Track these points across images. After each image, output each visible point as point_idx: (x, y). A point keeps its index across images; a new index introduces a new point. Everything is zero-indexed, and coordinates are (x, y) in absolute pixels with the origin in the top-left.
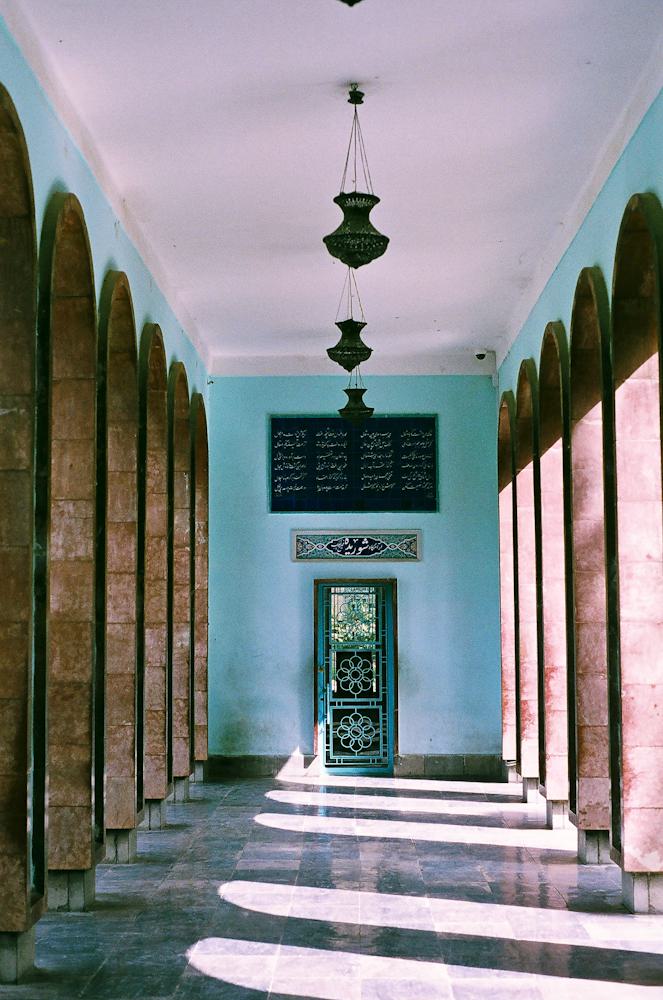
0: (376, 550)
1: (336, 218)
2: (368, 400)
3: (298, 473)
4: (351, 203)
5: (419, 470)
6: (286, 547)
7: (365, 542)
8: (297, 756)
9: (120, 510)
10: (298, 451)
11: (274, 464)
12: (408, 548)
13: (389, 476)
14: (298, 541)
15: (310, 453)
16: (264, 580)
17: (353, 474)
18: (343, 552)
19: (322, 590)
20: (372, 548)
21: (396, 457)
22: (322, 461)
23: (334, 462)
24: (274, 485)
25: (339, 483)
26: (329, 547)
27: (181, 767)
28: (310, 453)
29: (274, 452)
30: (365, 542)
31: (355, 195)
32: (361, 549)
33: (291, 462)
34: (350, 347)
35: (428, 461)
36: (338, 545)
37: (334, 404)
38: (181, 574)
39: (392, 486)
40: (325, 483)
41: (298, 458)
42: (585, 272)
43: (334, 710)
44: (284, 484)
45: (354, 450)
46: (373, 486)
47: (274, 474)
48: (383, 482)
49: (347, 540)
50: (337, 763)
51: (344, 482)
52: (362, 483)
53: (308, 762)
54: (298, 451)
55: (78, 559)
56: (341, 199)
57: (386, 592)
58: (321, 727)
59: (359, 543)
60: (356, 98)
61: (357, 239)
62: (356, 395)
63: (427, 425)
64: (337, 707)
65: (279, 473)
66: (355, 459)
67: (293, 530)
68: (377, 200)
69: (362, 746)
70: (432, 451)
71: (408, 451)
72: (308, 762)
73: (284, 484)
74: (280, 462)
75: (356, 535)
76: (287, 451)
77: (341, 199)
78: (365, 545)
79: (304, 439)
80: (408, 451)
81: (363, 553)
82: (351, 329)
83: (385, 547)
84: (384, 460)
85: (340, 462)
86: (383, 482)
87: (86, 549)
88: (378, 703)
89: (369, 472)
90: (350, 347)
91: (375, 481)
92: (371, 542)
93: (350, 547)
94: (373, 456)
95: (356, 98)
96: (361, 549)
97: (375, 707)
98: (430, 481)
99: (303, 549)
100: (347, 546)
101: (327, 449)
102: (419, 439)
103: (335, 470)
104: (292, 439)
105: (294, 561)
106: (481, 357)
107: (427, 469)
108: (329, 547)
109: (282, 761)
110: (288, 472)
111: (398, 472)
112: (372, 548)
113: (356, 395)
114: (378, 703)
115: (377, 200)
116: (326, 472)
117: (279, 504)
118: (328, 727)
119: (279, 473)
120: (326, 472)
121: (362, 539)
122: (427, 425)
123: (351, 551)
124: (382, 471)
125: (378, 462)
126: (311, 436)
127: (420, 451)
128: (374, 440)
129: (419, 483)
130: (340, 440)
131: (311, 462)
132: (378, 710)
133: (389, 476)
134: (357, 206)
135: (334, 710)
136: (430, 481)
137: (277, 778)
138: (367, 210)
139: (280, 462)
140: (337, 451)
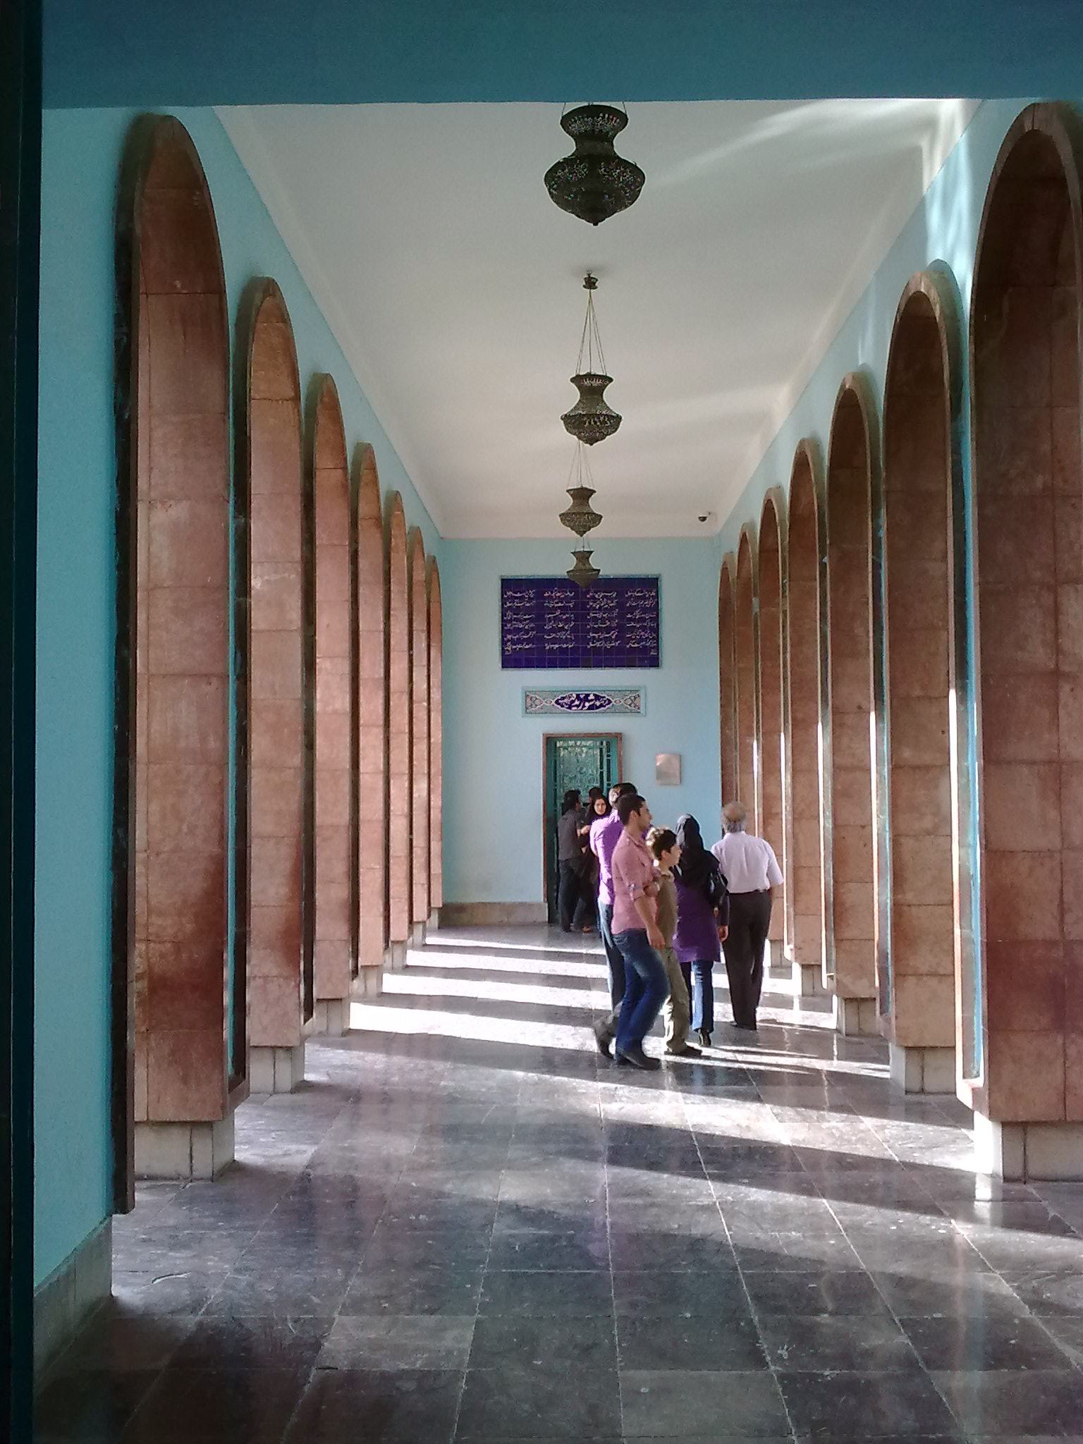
0: (601, 706)
1: (572, 397)
2: (594, 562)
4: (587, 383)
5: (644, 628)
7: (591, 697)
9: (371, 668)
10: (528, 611)
11: (504, 622)
12: (632, 702)
13: (614, 634)
15: (539, 614)
17: (580, 632)
18: (570, 708)
19: (551, 742)
21: (621, 616)
24: (504, 643)
25: (567, 641)
26: (557, 702)
27: (420, 912)
28: (539, 614)
30: (591, 697)
31: (590, 376)
32: (587, 704)
34: (581, 510)
37: (561, 566)
38: (420, 728)
40: (554, 641)
42: (802, 443)
45: (581, 611)
46: (598, 644)
47: (504, 632)
54: (528, 611)
55: (335, 712)
56: (577, 380)
59: (586, 698)
60: (590, 283)
61: (592, 419)
62: (583, 557)
63: (651, 584)
68: (611, 380)
70: (656, 609)
71: (632, 610)
76: (517, 611)
77: (577, 380)
80: (632, 610)
81: (590, 708)
82: (583, 495)
83: (610, 702)
85: (567, 621)
87: (344, 703)
89: (596, 631)
90: (581, 510)
93: (577, 703)
95: (590, 283)
96: (587, 704)
99: (531, 703)
101: (556, 609)
102: (643, 598)
104: (522, 598)
106: (703, 519)
108: (557, 702)
110: (518, 630)
111: (621, 629)
112: (598, 703)
113: (583, 557)
115: (611, 380)
116: (553, 630)
117: (511, 661)
119: (509, 632)
120: (553, 630)
122: (651, 584)
124: (608, 629)
125: (603, 620)
126: (540, 596)
127: (644, 610)
128: (601, 601)
130: (568, 599)
131: (540, 618)
133: (614, 634)
134: (591, 387)
138: (602, 388)
139: (511, 621)
140: (564, 609)
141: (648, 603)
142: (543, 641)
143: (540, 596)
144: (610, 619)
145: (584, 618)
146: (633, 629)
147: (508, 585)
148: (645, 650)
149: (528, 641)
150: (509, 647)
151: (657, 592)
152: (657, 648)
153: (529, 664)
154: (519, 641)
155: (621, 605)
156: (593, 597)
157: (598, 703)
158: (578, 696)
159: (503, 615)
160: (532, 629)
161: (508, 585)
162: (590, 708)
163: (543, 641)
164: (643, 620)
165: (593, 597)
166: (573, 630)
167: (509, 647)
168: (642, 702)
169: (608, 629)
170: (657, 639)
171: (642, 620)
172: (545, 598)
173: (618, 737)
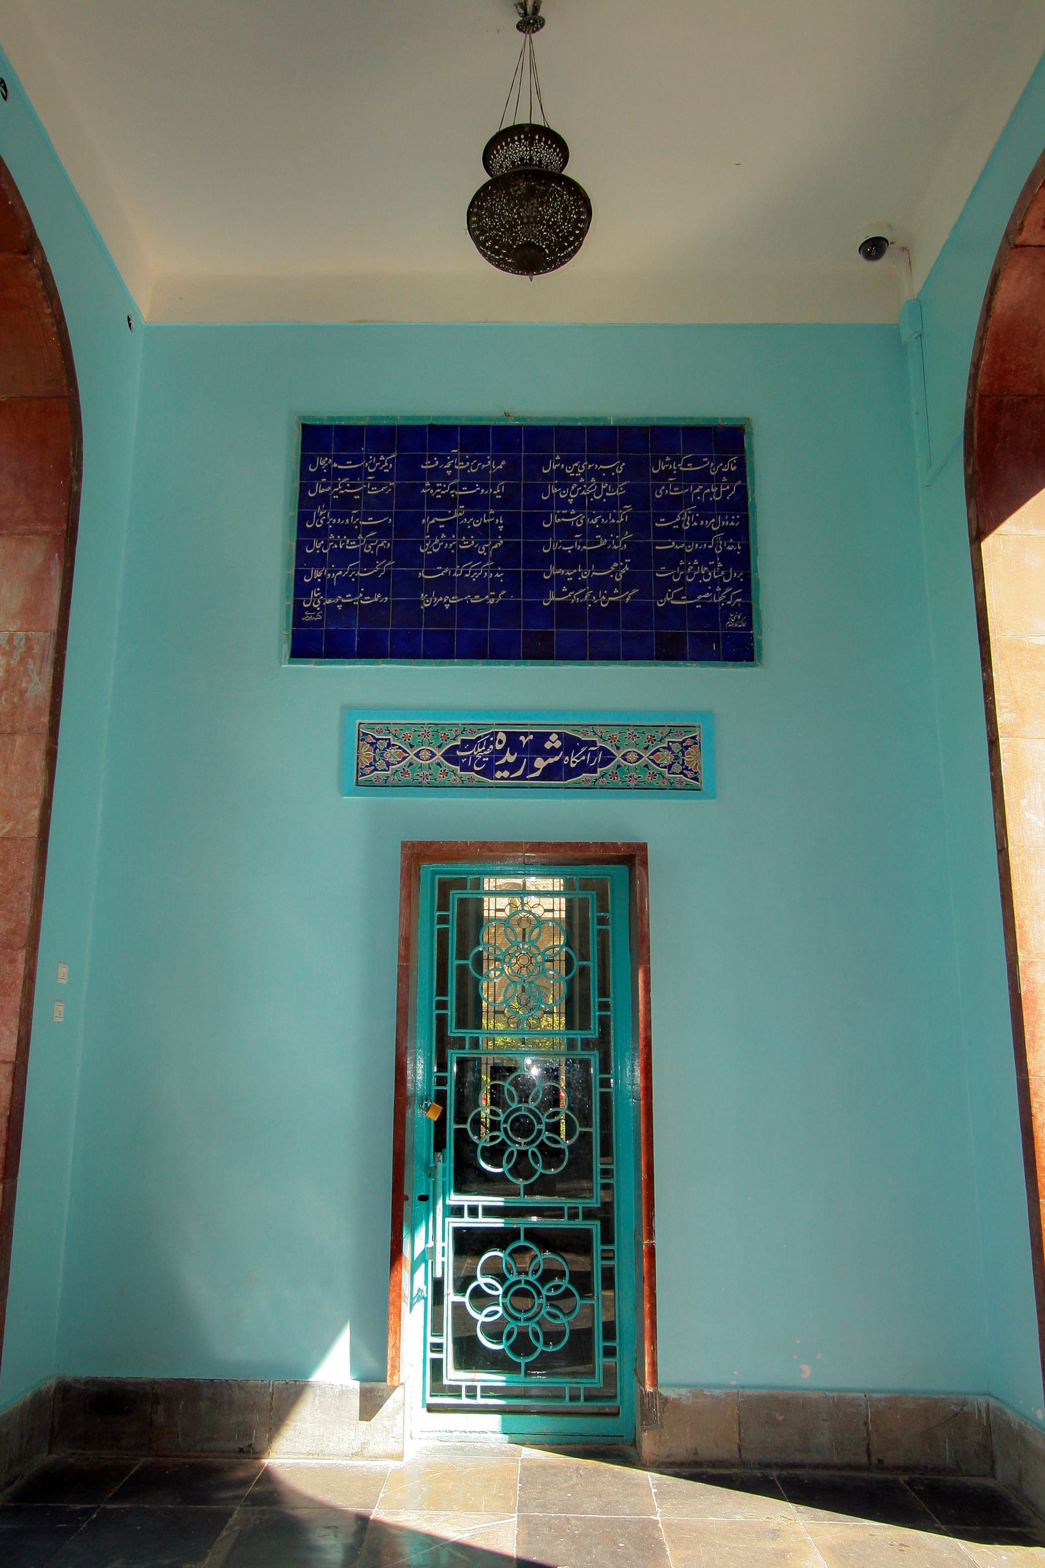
0: (583, 768)
3: (368, 561)
5: (704, 557)
6: (328, 754)
8: (335, 1370)
10: (376, 506)
12: (677, 761)
13: (619, 570)
14: (362, 737)
15: (405, 519)
16: (273, 845)
18: (488, 771)
19: (438, 887)
20: (573, 761)
21: (638, 524)
22: (435, 531)
23: (465, 532)
24: (301, 590)
28: (405, 519)
29: (306, 507)
32: (540, 763)
33: (350, 532)
35: (728, 533)
36: (478, 752)
39: (628, 597)
40: (445, 586)
41: (370, 522)
43: (457, 1231)
44: (327, 588)
46: (573, 597)
48: (598, 585)
49: (502, 737)
50: (465, 1401)
51: (496, 585)
52: (541, 587)
53: (371, 1403)
57: (610, 878)
58: (415, 1282)
64: (466, 1221)
65: (318, 560)
66: (529, 544)
67: (347, 709)
69: (540, 1346)
70: (738, 506)
72: (371, 1403)
73: (327, 588)
74: (320, 533)
75: (530, 723)
78: (554, 752)
79: (389, 477)
81: (549, 773)
83: (608, 757)
84: (606, 530)
85: (485, 533)
86: (598, 585)
88: (589, 1214)
89: (565, 560)
91: (582, 584)
92: (570, 744)
93: (510, 758)
94: (577, 520)
96: (540, 763)
97: (579, 1223)
98: (735, 584)
99: (375, 759)
100: (503, 752)
101: (449, 502)
102: (703, 477)
103: (471, 555)
104: (353, 474)
105: (350, 794)
107: (726, 556)
108: (451, 756)
109: (282, 1399)
110: (343, 557)
111: (639, 555)
114: (589, 1214)
116: (445, 558)
118: (438, 1286)
119: (318, 560)
120: (445, 558)
121: (546, 736)
122: (724, 444)
123: (512, 767)
124: (602, 559)
126: (410, 467)
127: (705, 508)
129: (703, 588)
131: (408, 527)
132: (588, 1233)
133: (619, 570)
135: (457, 1231)
136: (735, 584)
137: (266, 1462)
139: (320, 533)
141: (715, 492)
142: (417, 585)
143: (410, 467)
144: (606, 530)
145: (533, 524)
146: (672, 559)
147: (316, 438)
148: (710, 613)
149: (371, 586)
150: (316, 599)
151: (741, 464)
152: (747, 610)
153: (371, 649)
154: (346, 586)
155: (637, 497)
156: (560, 474)
157: (573, 761)
158: (513, 739)
159: (303, 517)
160: (384, 554)
161: (316, 438)
162: (549, 773)
163: (417, 585)
164: (705, 534)
165: (560, 474)
166: (500, 559)
167: (316, 599)
168: (702, 760)
169: (602, 559)
170: (745, 585)
171: (701, 534)
172: (422, 475)
173: (631, 858)
